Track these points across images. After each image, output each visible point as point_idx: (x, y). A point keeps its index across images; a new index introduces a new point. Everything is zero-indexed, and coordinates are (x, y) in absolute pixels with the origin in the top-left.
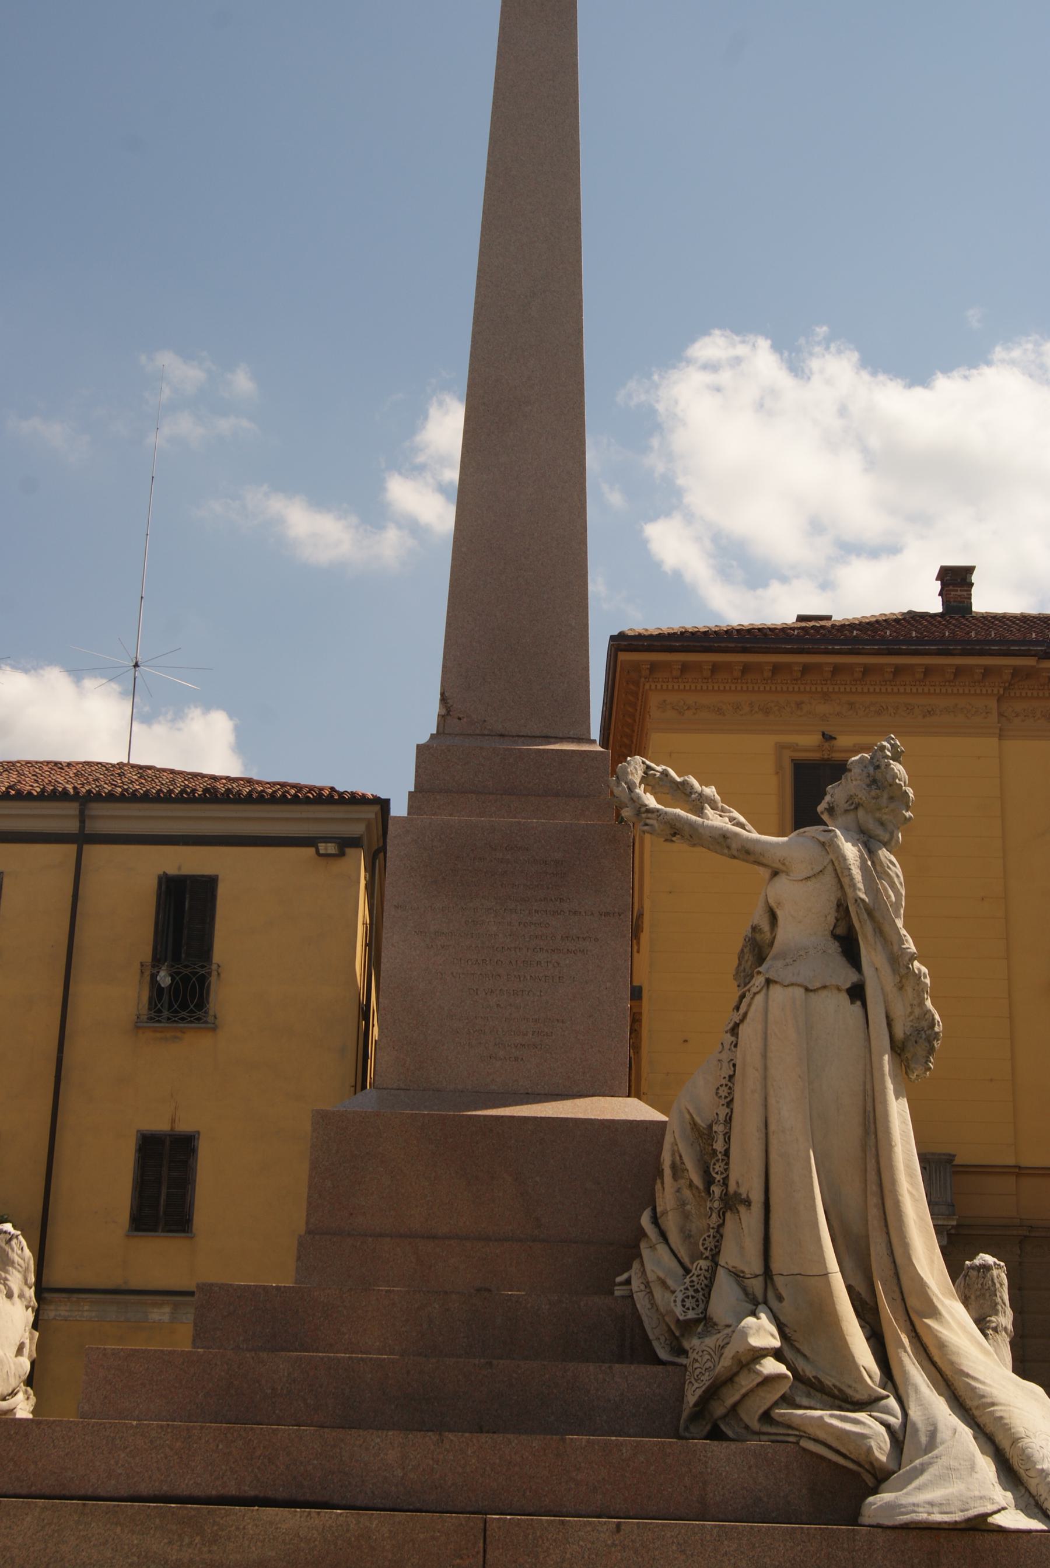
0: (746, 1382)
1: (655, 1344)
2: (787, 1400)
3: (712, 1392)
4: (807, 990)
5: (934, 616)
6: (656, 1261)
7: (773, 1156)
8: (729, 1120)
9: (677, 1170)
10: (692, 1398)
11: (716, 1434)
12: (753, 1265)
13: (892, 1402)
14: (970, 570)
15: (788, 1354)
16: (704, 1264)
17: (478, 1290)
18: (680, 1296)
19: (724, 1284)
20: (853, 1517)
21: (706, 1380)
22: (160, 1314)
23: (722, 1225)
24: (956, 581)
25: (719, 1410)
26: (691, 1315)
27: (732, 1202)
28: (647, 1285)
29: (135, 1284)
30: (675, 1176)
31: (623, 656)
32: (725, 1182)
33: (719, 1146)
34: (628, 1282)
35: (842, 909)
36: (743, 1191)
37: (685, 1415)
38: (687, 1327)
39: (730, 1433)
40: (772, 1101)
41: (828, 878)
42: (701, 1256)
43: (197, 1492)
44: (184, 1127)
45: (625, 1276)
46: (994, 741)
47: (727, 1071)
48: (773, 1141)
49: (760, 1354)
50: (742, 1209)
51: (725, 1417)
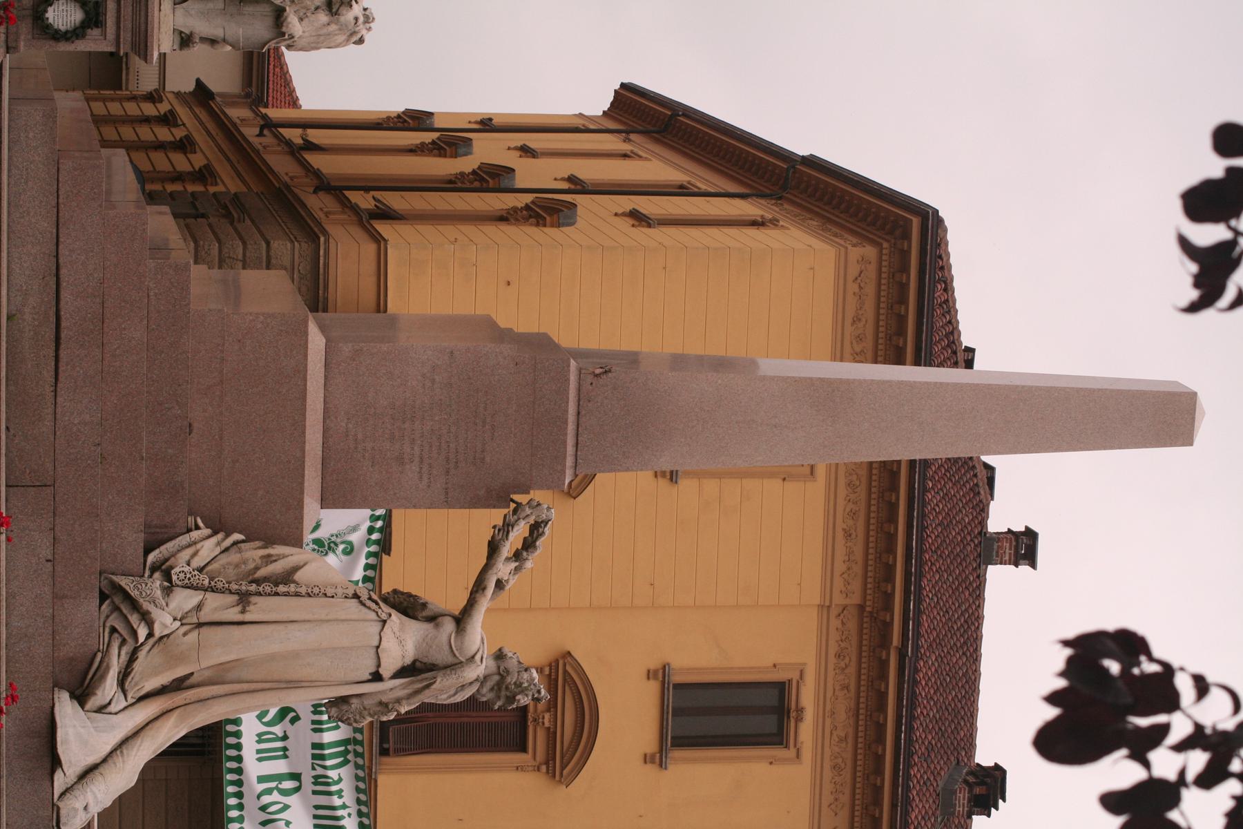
0: (134, 619)
1: (157, 551)
2: (124, 642)
3: (127, 597)
4: (378, 647)
5: (983, 523)
7: (272, 627)
8: (297, 595)
9: (268, 559)
10: (124, 582)
11: (103, 597)
12: (205, 616)
13: (124, 704)
14: (1033, 565)
15: (151, 641)
16: (206, 582)
17: (190, 425)
18: (187, 569)
20: (57, 685)
21: (134, 593)
23: (231, 592)
24: (1023, 548)
25: (117, 600)
26: (174, 578)
27: (244, 599)
28: (195, 543)
30: (262, 557)
31: (916, 222)
32: (260, 594)
33: (282, 589)
34: (197, 528)
35: (432, 668)
36: (251, 608)
37: (114, 577)
38: (167, 576)
39: (104, 607)
40: (307, 626)
41: (450, 660)
42: (211, 579)
43: (62, 303)
45: (201, 524)
46: (817, 601)
47: (330, 592)
48: (281, 627)
49: (150, 624)
50: (239, 608)
51: (113, 602)
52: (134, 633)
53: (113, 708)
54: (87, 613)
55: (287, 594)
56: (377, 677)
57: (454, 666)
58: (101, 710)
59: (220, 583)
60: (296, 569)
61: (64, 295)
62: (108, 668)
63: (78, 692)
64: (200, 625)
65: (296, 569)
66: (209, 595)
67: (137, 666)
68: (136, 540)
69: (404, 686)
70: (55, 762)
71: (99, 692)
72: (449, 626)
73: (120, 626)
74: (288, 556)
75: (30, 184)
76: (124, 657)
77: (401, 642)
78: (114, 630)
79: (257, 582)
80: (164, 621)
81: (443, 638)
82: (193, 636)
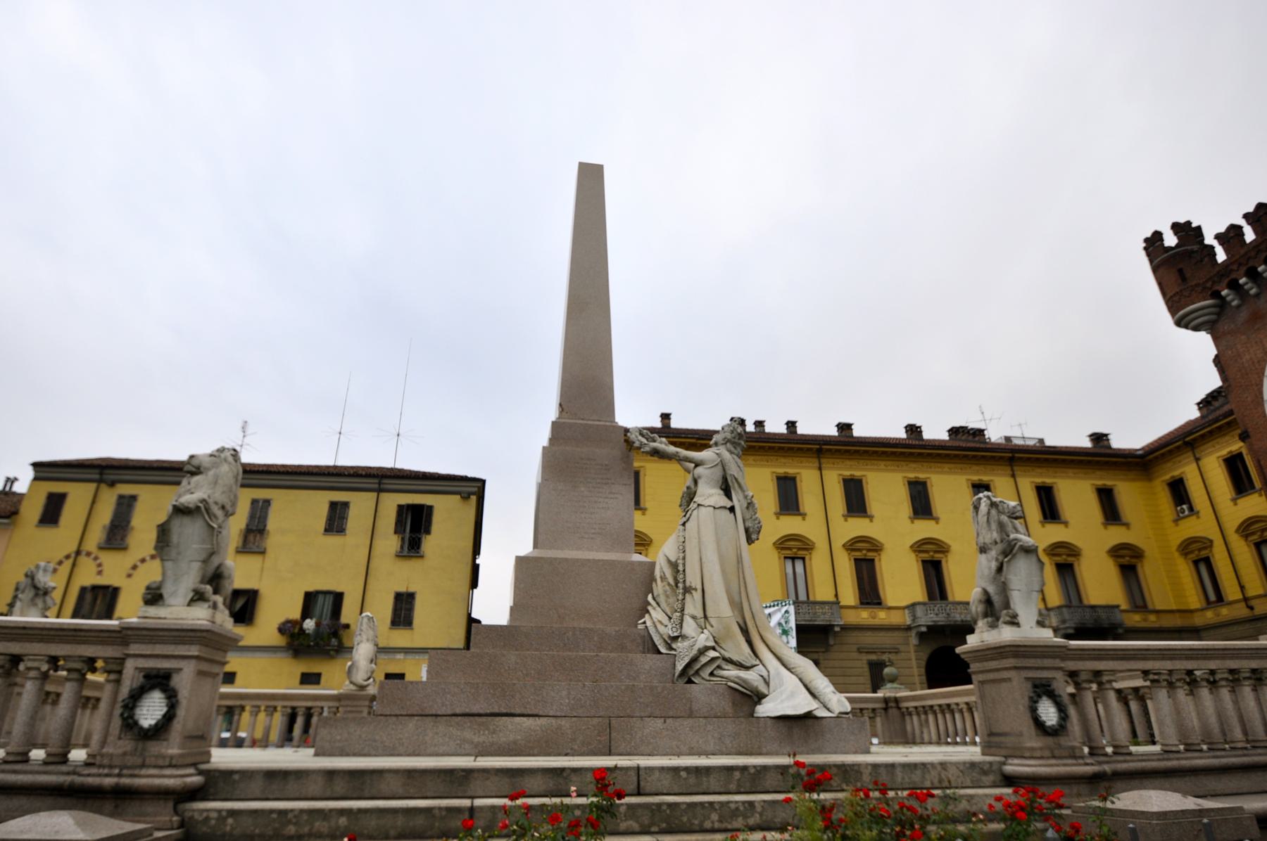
0: (704, 660)
2: (719, 667)
3: (688, 666)
6: (656, 614)
8: (684, 558)
9: (663, 578)
10: (680, 667)
11: (690, 682)
12: (700, 614)
19: (688, 620)
21: (687, 660)
22: (400, 656)
24: (666, 417)
27: (687, 590)
29: (392, 645)
33: (681, 568)
35: (725, 480)
38: (675, 639)
41: (720, 467)
43: (481, 712)
44: (411, 590)
49: (707, 649)
52: (713, 659)
53: (765, 674)
54: (700, 691)
55: (684, 565)
56: (732, 509)
57: (723, 465)
58: (767, 683)
59: (678, 606)
60: (669, 561)
61: (475, 710)
62: (738, 677)
63: (756, 699)
64: (705, 617)
65: (669, 561)
66: (686, 612)
67: (735, 658)
68: (651, 661)
69: (737, 493)
70: (809, 716)
71: (755, 684)
72: (700, 470)
73: (709, 670)
74: (661, 568)
75: (377, 738)
76: (730, 667)
77: (710, 496)
78: (712, 674)
79: (677, 583)
80: (703, 639)
81: (707, 472)
82: (713, 621)
